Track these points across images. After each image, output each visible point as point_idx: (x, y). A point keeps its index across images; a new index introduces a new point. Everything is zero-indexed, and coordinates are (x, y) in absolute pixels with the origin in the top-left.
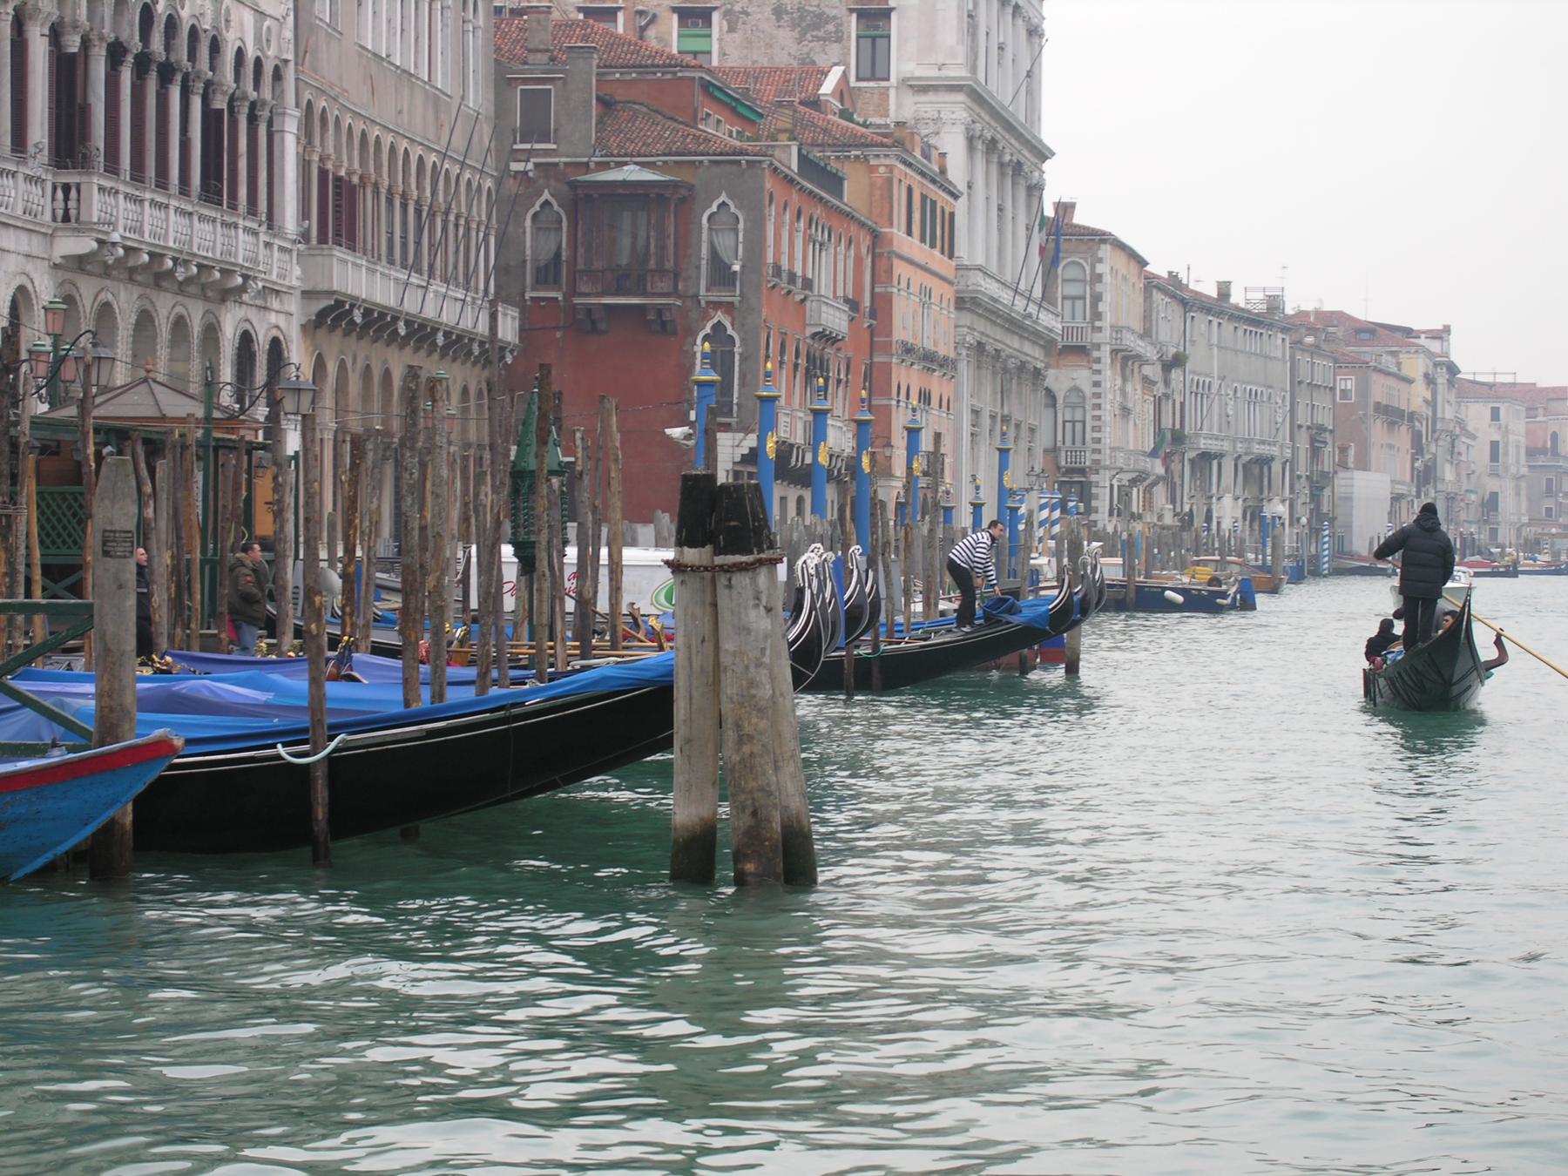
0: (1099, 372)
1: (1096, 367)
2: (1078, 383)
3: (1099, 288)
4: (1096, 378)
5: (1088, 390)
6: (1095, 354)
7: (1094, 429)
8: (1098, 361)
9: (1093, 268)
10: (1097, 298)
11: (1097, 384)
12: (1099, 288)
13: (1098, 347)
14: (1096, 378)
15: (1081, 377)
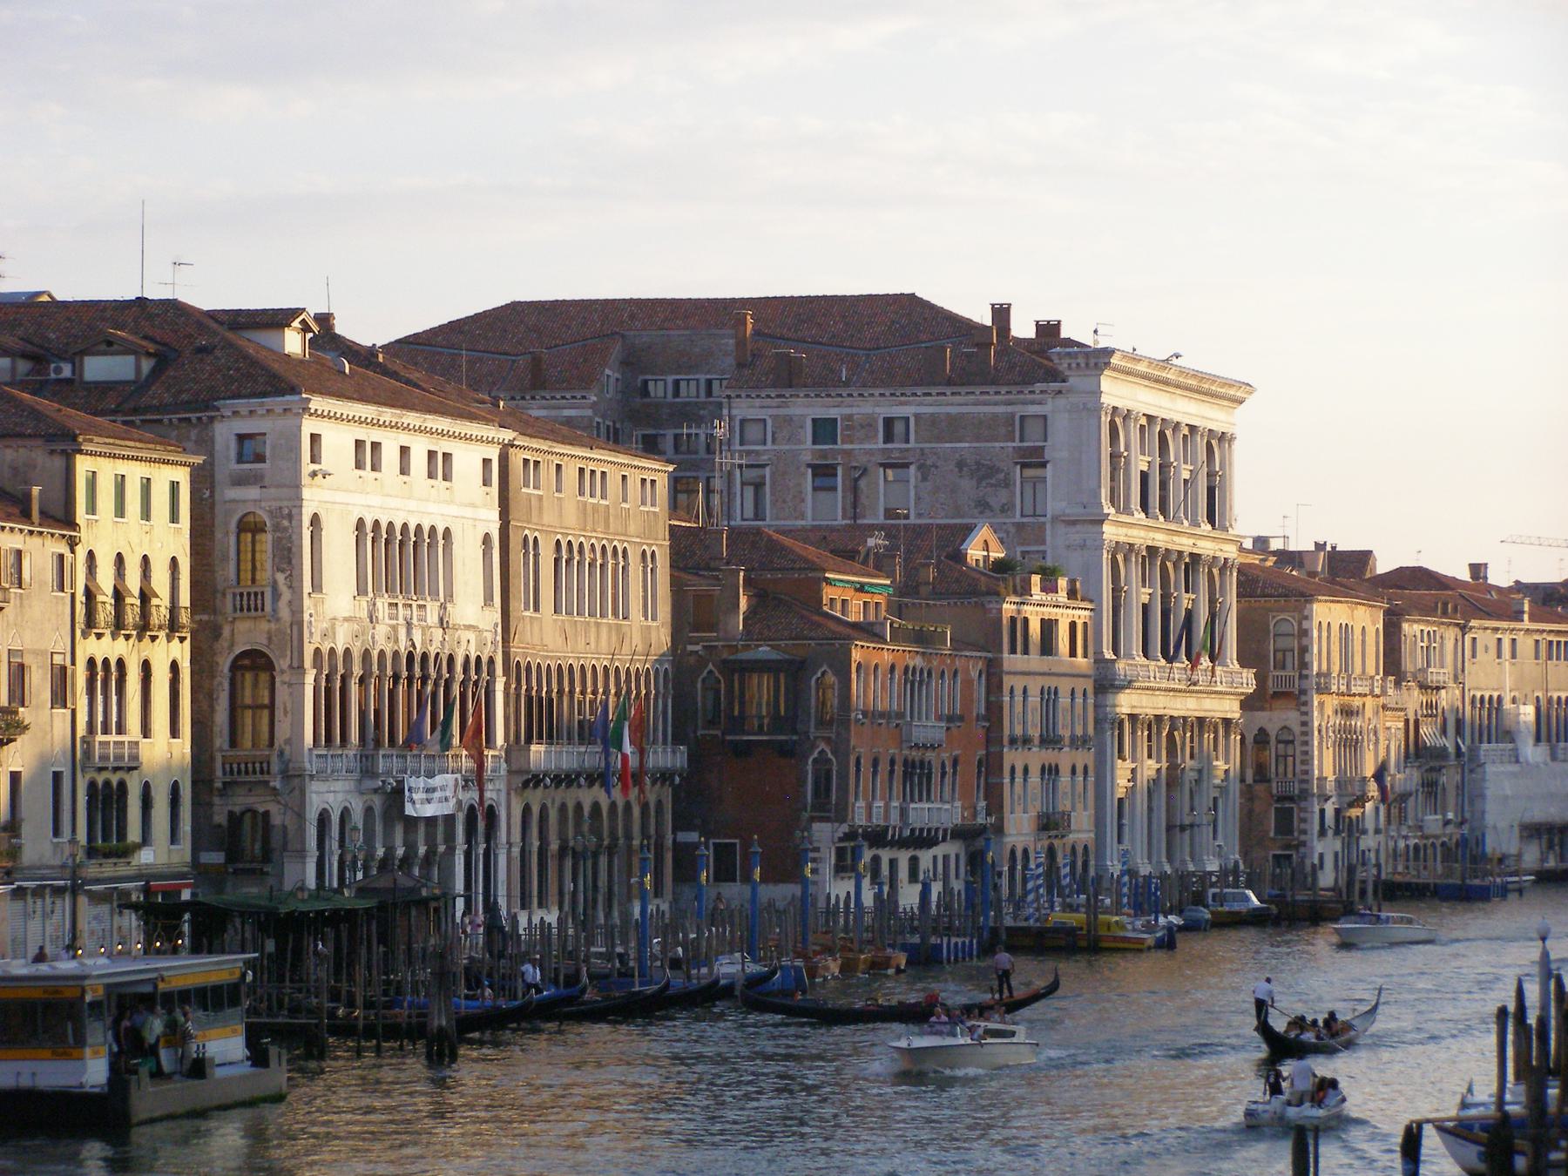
0: (1306, 713)
1: (1303, 709)
2: (1287, 723)
3: (1305, 641)
4: (1304, 718)
5: (1297, 729)
6: (1303, 698)
7: (1303, 762)
8: (1305, 704)
9: (1300, 624)
10: (1304, 650)
11: (1304, 724)
12: (1305, 641)
13: (1303, 692)
14: (1304, 718)
15: (1291, 717)
